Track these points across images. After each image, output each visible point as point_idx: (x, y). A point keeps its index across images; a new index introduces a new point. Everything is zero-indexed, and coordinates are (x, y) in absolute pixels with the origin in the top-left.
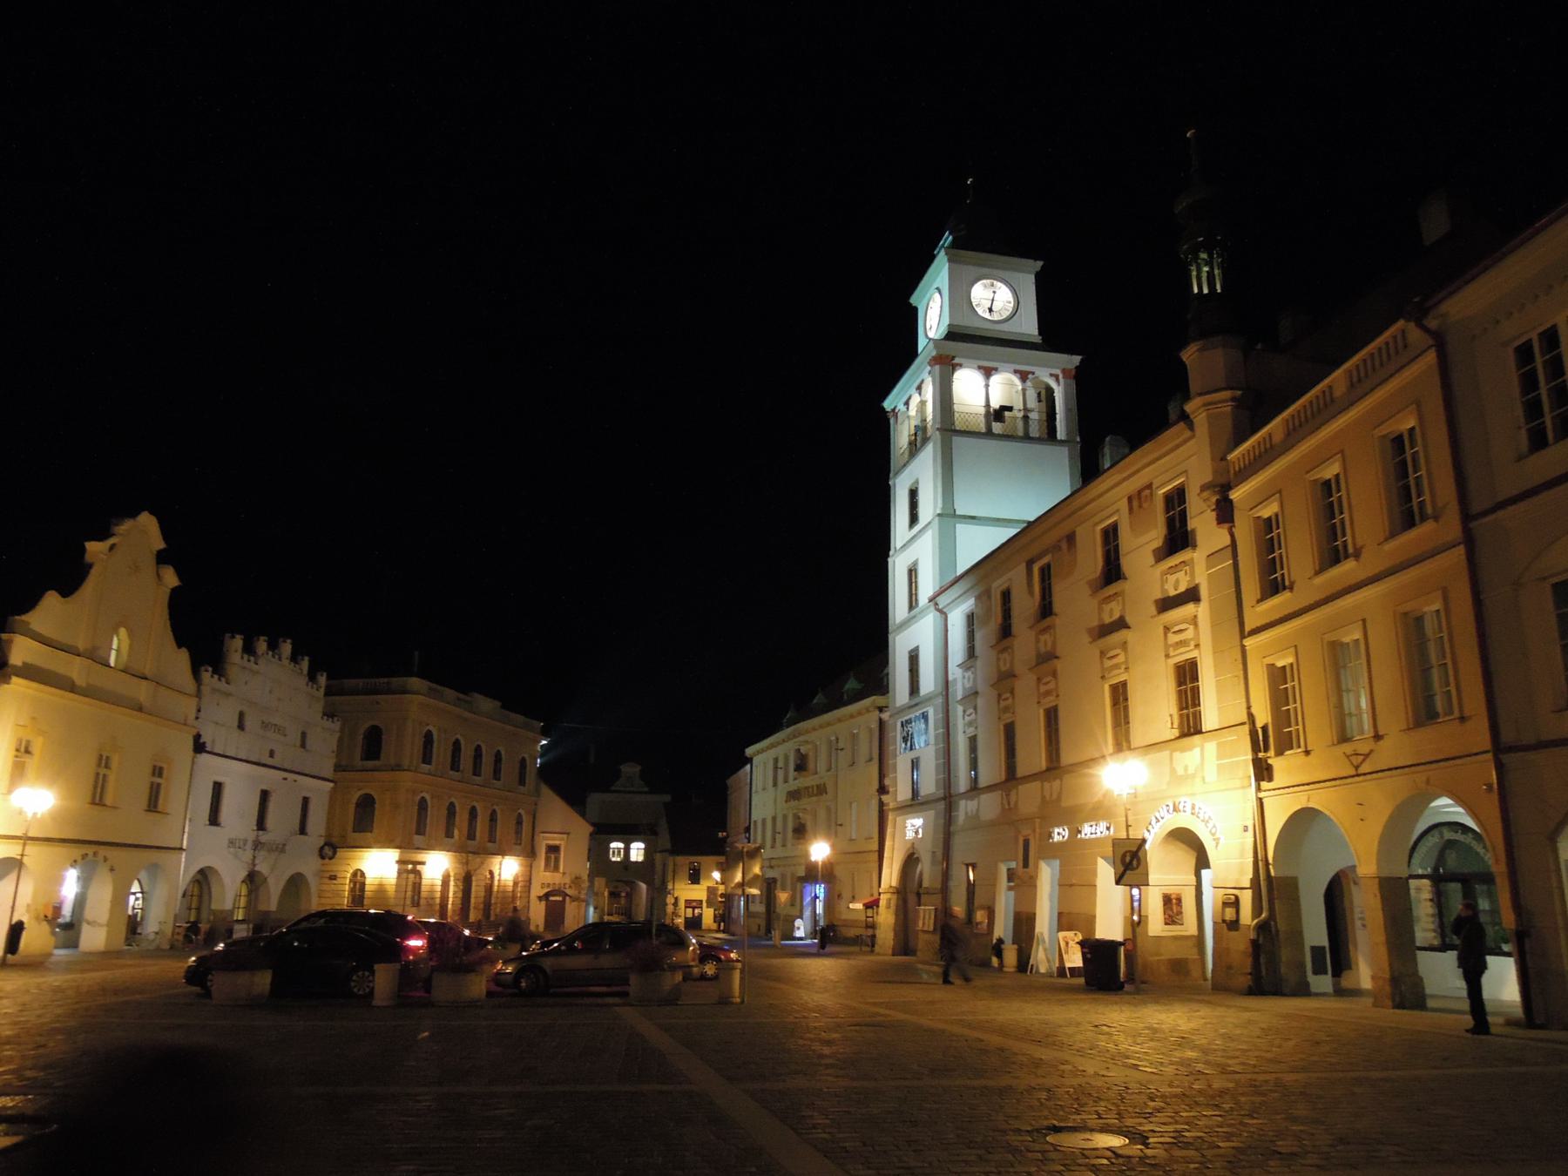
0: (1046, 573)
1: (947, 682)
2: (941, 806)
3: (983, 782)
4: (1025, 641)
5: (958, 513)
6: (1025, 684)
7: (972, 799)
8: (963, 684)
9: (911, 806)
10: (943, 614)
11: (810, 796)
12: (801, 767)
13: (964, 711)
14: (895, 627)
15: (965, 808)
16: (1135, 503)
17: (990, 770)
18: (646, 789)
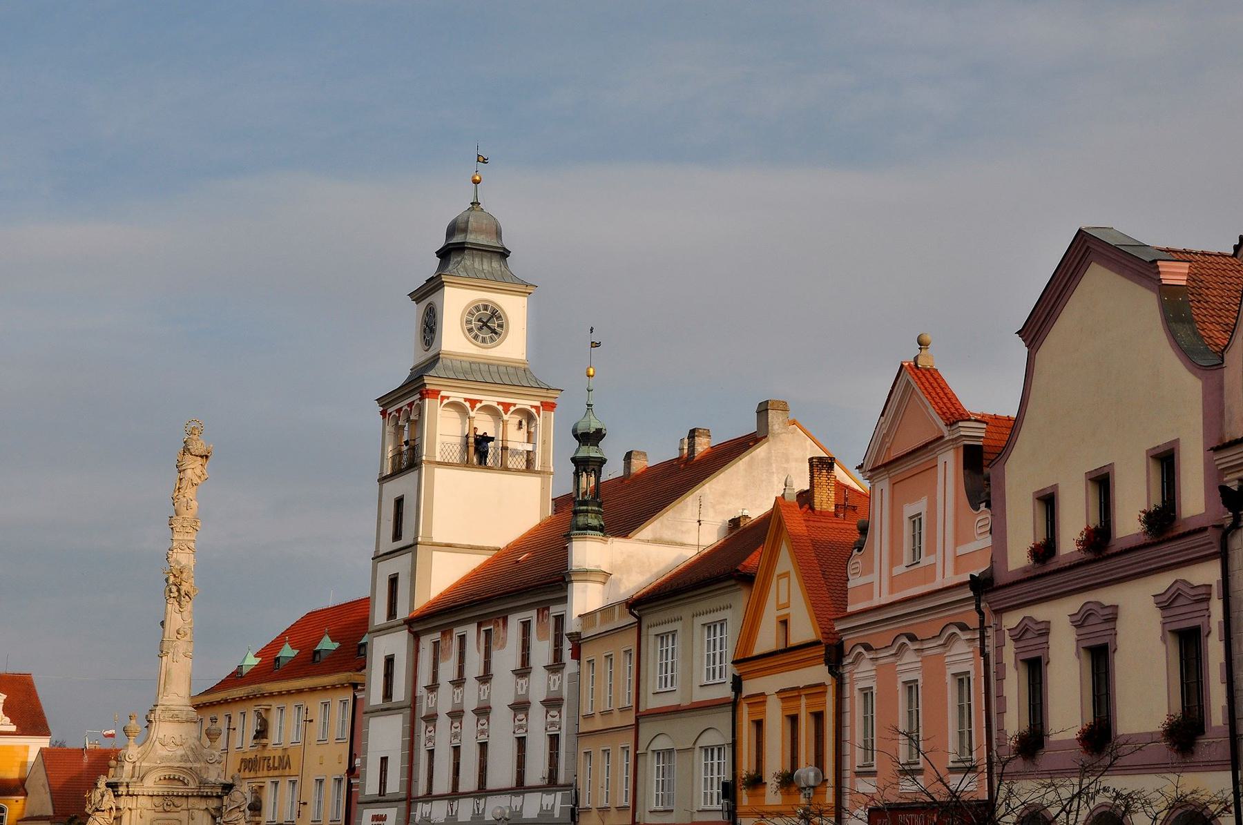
0: (488, 632)
1: (416, 697)
2: (403, 805)
3: (436, 792)
4: (471, 683)
5: (437, 538)
6: (469, 719)
7: (426, 802)
8: (428, 704)
9: (377, 801)
10: (416, 637)
11: (269, 768)
12: (262, 733)
13: (427, 728)
14: (374, 629)
15: (421, 810)
16: (540, 617)
17: (442, 784)
18: (13, 728)
